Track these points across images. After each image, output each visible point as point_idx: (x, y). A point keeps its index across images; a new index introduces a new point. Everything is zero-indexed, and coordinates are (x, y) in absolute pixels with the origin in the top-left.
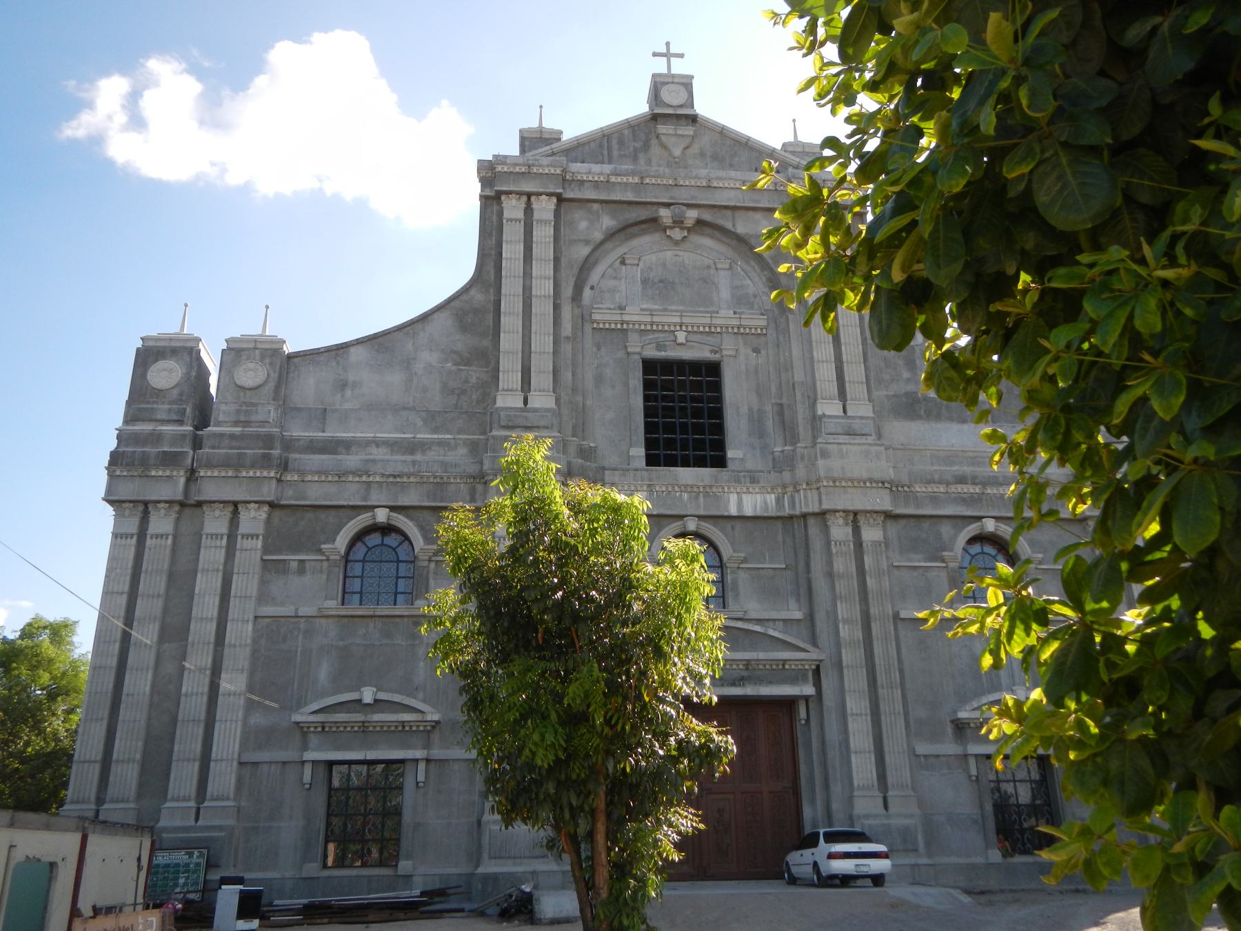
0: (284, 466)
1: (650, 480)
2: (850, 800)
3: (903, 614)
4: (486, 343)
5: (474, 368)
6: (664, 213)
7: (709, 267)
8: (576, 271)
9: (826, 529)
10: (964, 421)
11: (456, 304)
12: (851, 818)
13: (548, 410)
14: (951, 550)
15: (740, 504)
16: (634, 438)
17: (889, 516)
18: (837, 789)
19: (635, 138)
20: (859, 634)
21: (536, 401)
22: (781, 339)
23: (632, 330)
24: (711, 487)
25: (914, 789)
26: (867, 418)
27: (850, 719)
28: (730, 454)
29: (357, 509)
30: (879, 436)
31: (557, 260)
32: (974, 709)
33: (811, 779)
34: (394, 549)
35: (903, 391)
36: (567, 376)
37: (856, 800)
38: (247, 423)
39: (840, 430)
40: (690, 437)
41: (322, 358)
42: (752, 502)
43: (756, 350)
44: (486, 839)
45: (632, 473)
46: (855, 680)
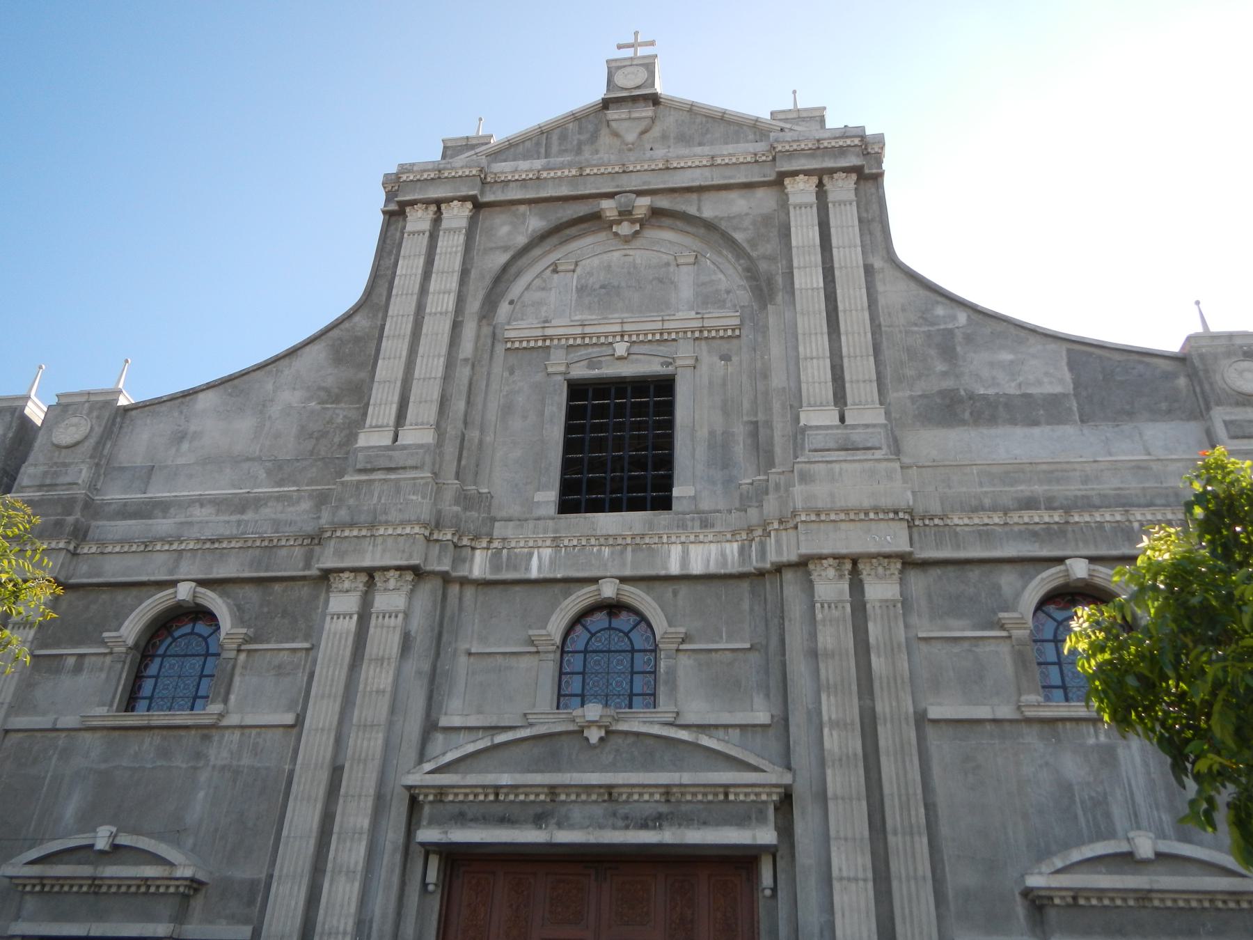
0: (80, 534)
1: (556, 531)
3: (934, 713)
4: (363, 375)
5: (343, 405)
6: (606, 204)
7: (668, 264)
8: (488, 281)
9: (809, 586)
10: (1035, 423)
11: (335, 333)
13: (421, 446)
14: (1015, 610)
16: (544, 480)
17: (908, 563)
19: (581, 130)
20: (856, 744)
21: (409, 437)
22: (760, 339)
23: (557, 347)
24: (643, 536)
26: (874, 426)
28: (676, 492)
29: (161, 585)
30: (896, 449)
31: (465, 273)
32: (1058, 872)
34: (205, 639)
35: (936, 389)
36: (459, 405)
38: (53, 486)
39: (832, 445)
40: (626, 475)
41: (164, 408)
42: (702, 556)
43: (726, 358)
45: (531, 524)
46: (848, 819)
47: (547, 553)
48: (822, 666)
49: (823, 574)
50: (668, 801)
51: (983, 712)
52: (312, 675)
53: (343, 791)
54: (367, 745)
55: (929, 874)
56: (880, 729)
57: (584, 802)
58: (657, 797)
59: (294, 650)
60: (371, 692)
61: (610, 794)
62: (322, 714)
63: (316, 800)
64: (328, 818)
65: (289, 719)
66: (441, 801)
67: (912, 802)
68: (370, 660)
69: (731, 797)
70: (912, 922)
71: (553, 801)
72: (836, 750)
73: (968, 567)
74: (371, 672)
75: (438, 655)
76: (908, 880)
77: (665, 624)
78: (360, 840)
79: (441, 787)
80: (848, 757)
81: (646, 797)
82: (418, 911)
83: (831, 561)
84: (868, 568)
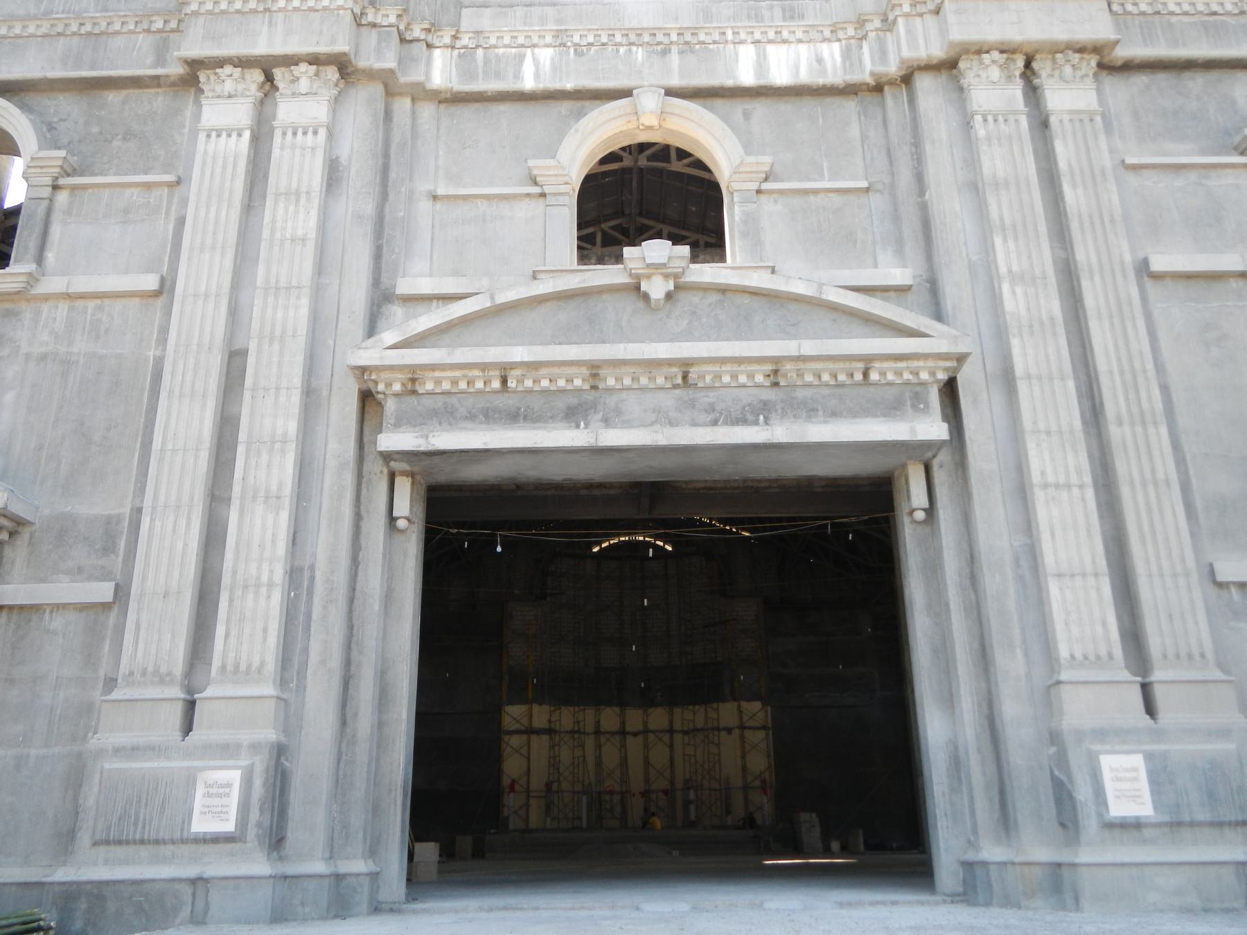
1: (560, 21)
2: (1049, 693)
3: (1159, 263)
12: (1054, 737)
15: (761, 64)
18: (1012, 665)
20: (1053, 306)
25: (1221, 666)
27: (1039, 496)
33: (943, 649)
37: (1066, 692)
44: (91, 796)
46: (1050, 406)
47: (546, 55)
48: (991, 200)
49: (983, 74)
50: (776, 384)
51: (1230, 262)
52: (181, 222)
53: (249, 381)
54: (281, 318)
55: (1173, 476)
56: (1086, 284)
57: (643, 389)
58: (760, 378)
59: (148, 186)
60: (282, 241)
61: (685, 377)
62: (204, 273)
63: (204, 396)
64: (226, 427)
65: (150, 282)
66: (414, 392)
67: (1140, 380)
68: (277, 195)
69: (874, 376)
70: (1155, 541)
71: (594, 387)
72: (1023, 312)
73: (1187, 74)
74: (281, 212)
75: (384, 196)
76: (1144, 485)
77: (741, 151)
78: (283, 451)
79: (413, 369)
80: (1042, 323)
81: (743, 379)
82: (384, 556)
83: (995, 55)
84: (1049, 64)
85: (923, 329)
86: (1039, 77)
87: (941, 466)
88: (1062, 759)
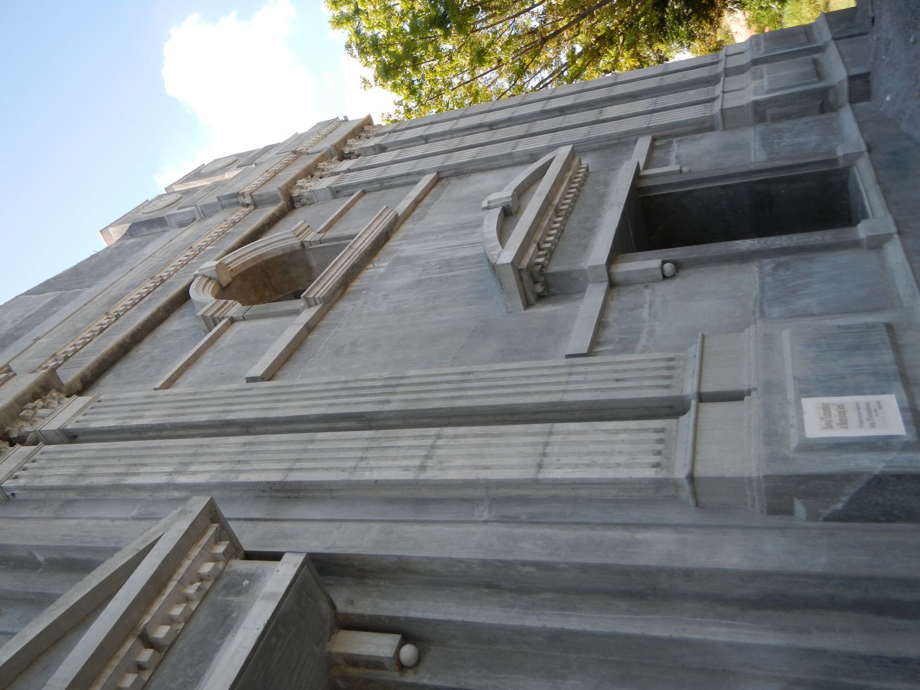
2: (703, 496)
69: (162, 632)
85: (142, 547)
86: (29, 433)
87: (351, 603)
88: (814, 487)
